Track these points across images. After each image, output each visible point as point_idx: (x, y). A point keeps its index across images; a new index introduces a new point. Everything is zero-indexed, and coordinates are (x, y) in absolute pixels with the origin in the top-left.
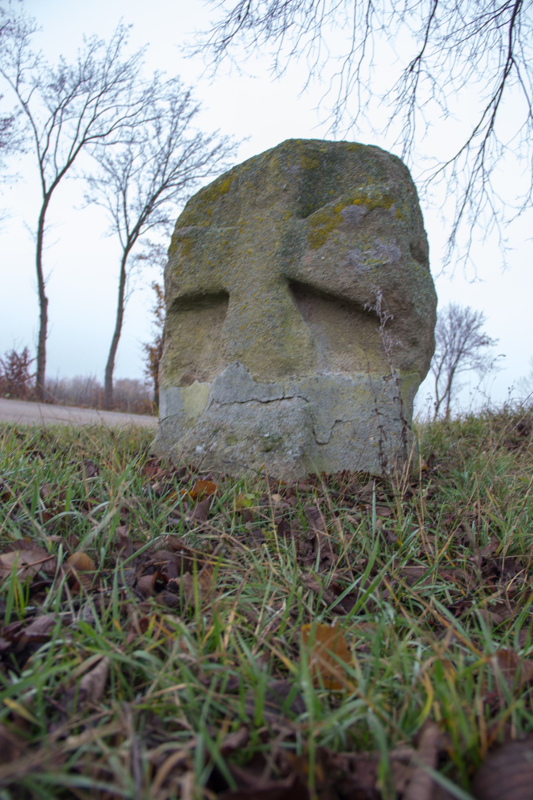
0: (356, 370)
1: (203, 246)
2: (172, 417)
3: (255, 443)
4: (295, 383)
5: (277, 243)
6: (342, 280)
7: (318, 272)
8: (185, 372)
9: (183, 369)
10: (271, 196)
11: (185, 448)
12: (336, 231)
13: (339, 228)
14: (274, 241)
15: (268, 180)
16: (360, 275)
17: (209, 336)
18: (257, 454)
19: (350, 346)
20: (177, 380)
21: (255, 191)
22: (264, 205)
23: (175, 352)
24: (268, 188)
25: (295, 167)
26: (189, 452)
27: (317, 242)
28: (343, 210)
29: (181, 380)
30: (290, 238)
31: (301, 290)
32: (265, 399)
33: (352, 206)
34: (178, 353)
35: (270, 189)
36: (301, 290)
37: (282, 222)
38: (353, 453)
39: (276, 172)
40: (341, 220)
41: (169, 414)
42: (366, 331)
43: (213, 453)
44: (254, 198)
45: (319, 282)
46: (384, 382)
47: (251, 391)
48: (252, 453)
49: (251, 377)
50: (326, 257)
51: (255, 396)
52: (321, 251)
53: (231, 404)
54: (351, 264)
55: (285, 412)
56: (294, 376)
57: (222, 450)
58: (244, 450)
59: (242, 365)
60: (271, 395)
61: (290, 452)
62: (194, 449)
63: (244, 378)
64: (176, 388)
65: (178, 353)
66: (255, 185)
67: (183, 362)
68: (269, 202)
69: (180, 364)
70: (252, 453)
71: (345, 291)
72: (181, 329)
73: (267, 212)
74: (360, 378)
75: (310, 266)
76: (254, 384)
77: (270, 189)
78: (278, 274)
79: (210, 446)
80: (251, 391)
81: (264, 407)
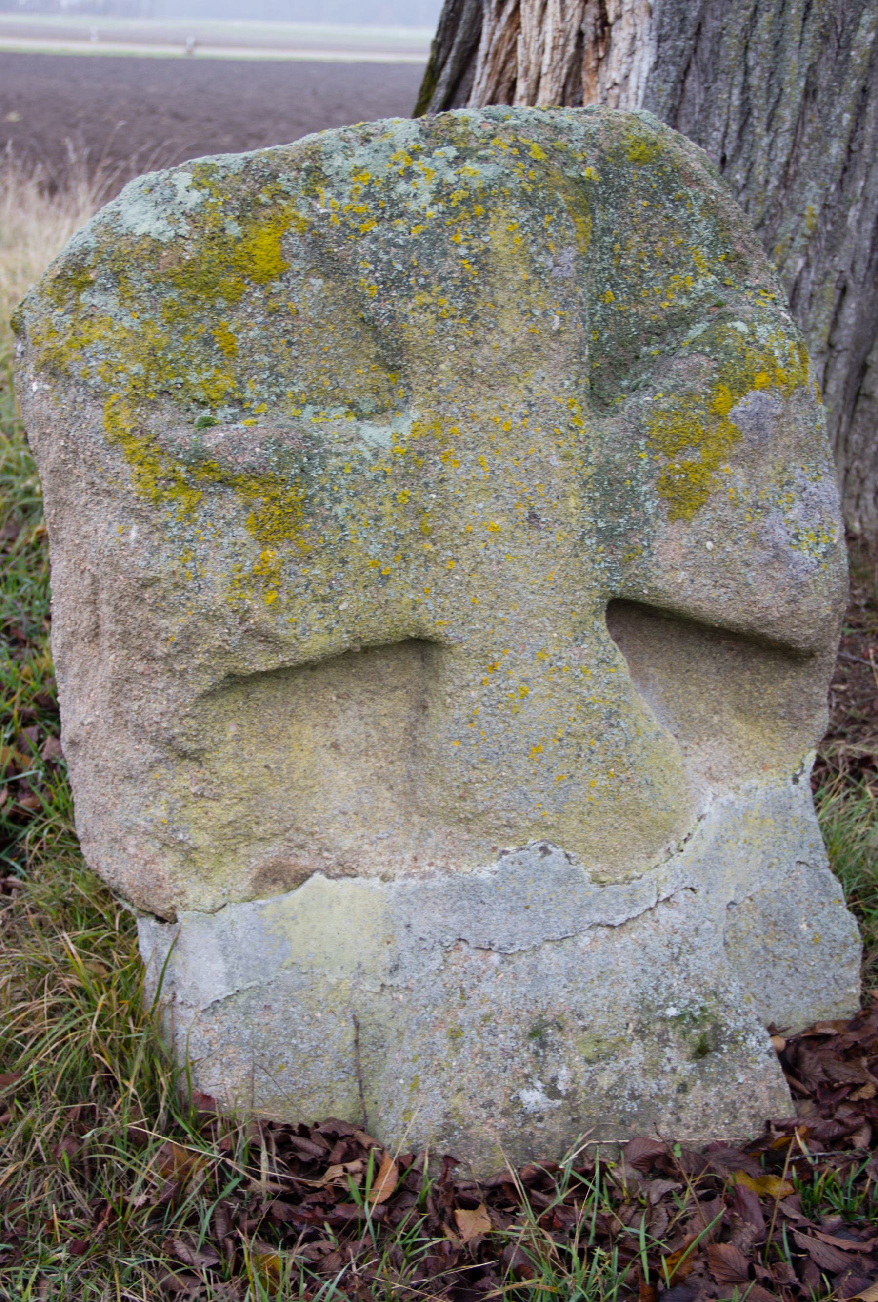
0: (738, 775)
1: (339, 510)
2: (258, 992)
3: (664, 1041)
4: (677, 861)
5: (572, 502)
7: (700, 580)
9: (260, 848)
10: (520, 350)
12: (726, 467)
13: (735, 460)
15: (501, 297)
17: (335, 746)
18: (686, 1068)
19: (716, 718)
20: (245, 886)
21: (466, 333)
22: (499, 376)
23: (228, 808)
24: (506, 325)
25: (568, 255)
26: (505, 1113)
27: (683, 498)
28: (737, 409)
30: (610, 490)
31: (634, 615)
32: (620, 919)
33: (752, 394)
34: (241, 808)
35: (513, 326)
36: (634, 615)
37: (572, 437)
38: (779, 972)
40: (735, 437)
41: (239, 984)
42: (752, 682)
43: (571, 1096)
44: (467, 353)
45: (706, 606)
46: (793, 787)
48: (674, 1070)
49: (587, 875)
50: (719, 544)
51: (597, 918)
55: (678, 938)
57: (592, 1083)
58: (653, 1069)
59: (557, 852)
60: (634, 903)
61: (752, 1042)
62: (517, 1102)
63: (567, 880)
64: (248, 906)
65: (241, 808)
66: (467, 311)
67: (259, 831)
68: (515, 368)
69: (248, 836)
70: (674, 1070)
71: (769, 624)
72: (238, 739)
73: (513, 398)
74: (748, 792)
75: (678, 568)
76: (595, 888)
77: (513, 326)
79: (554, 1080)
81: (628, 938)
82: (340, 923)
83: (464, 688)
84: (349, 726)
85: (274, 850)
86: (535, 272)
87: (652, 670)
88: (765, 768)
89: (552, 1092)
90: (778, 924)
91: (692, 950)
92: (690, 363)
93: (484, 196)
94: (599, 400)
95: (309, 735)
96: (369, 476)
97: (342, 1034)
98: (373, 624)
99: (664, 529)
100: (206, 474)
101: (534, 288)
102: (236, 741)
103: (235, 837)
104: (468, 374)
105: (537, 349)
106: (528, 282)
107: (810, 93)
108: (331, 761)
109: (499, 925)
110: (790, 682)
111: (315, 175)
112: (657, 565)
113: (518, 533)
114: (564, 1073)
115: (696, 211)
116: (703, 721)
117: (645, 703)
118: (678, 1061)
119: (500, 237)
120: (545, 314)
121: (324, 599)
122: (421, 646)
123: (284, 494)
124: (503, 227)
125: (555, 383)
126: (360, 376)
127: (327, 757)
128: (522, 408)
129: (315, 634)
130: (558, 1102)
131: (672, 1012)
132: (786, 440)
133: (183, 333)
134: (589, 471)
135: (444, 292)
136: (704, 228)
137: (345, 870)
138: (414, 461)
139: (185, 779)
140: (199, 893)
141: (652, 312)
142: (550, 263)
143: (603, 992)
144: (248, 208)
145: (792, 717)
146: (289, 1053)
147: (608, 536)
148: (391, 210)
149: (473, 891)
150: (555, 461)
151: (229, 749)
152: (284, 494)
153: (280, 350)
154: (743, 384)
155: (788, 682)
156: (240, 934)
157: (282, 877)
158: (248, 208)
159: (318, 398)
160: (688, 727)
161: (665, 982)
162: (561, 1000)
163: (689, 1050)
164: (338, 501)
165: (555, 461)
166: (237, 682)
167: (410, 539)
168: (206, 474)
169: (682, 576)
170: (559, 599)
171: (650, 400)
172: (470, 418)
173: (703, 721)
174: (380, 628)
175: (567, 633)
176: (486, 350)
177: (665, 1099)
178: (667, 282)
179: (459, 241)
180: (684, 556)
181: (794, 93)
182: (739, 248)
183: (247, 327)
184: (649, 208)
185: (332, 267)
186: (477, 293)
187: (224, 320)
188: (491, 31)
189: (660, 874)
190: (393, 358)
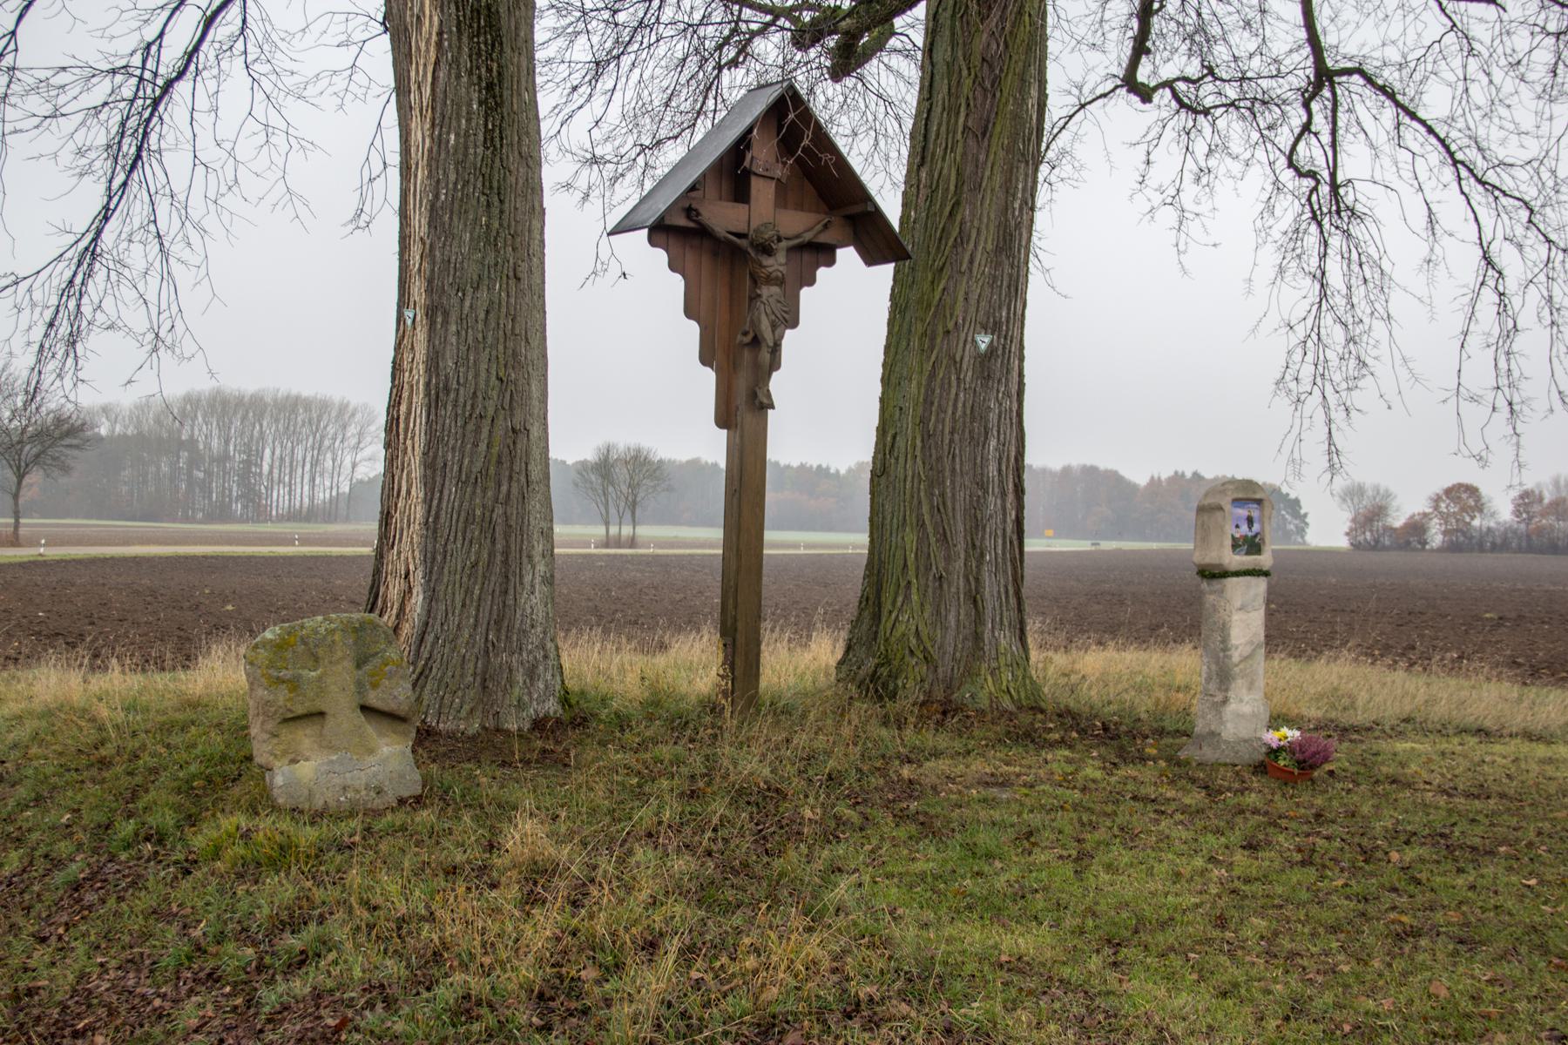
8: (292, 756)
22: (338, 662)
27: (375, 686)
31: (366, 709)
35: (339, 654)
36: (366, 709)
75: (373, 699)
77: (339, 654)
82: (306, 770)
83: (330, 722)
84: (308, 731)
90: (402, 776)
92: (377, 661)
93: (334, 630)
94: (358, 666)
95: (300, 733)
97: (306, 792)
100: (280, 681)
102: (284, 730)
103: (285, 753)
107: (463, 605)
108: (304, 737)
109: (337, 768)
110: (402, 727)
111: (302, 627)
117: (370, 729)
118: (373, 794)
119: (337, 637)
122: (322, 714)
123: (294, 684)
125: (348, 664)
126: (310, 664)
129: (300, 710)
137: (307, 760)
138: (320, 679)
139: (275, 741)
140: (278, 764)
141: (372, 651)
144: (289, 634)
145: (405, 734)
148: (316, 633)
149: (332, 762)
152: (294, 684)
157: (294, 761)
158: (289, 634)
159: (303, 668)
160: (381, 734)
162: (349, 782)
166: (286, 720)
168: (280, 681)
171: (367, 668)
174: (313, 710)
179: (329, 638)
181: (459, 606)
183: (289, 655)
185: (305, 644)
188: (382, 589)
189: (371, 759)
190: (317, 659)
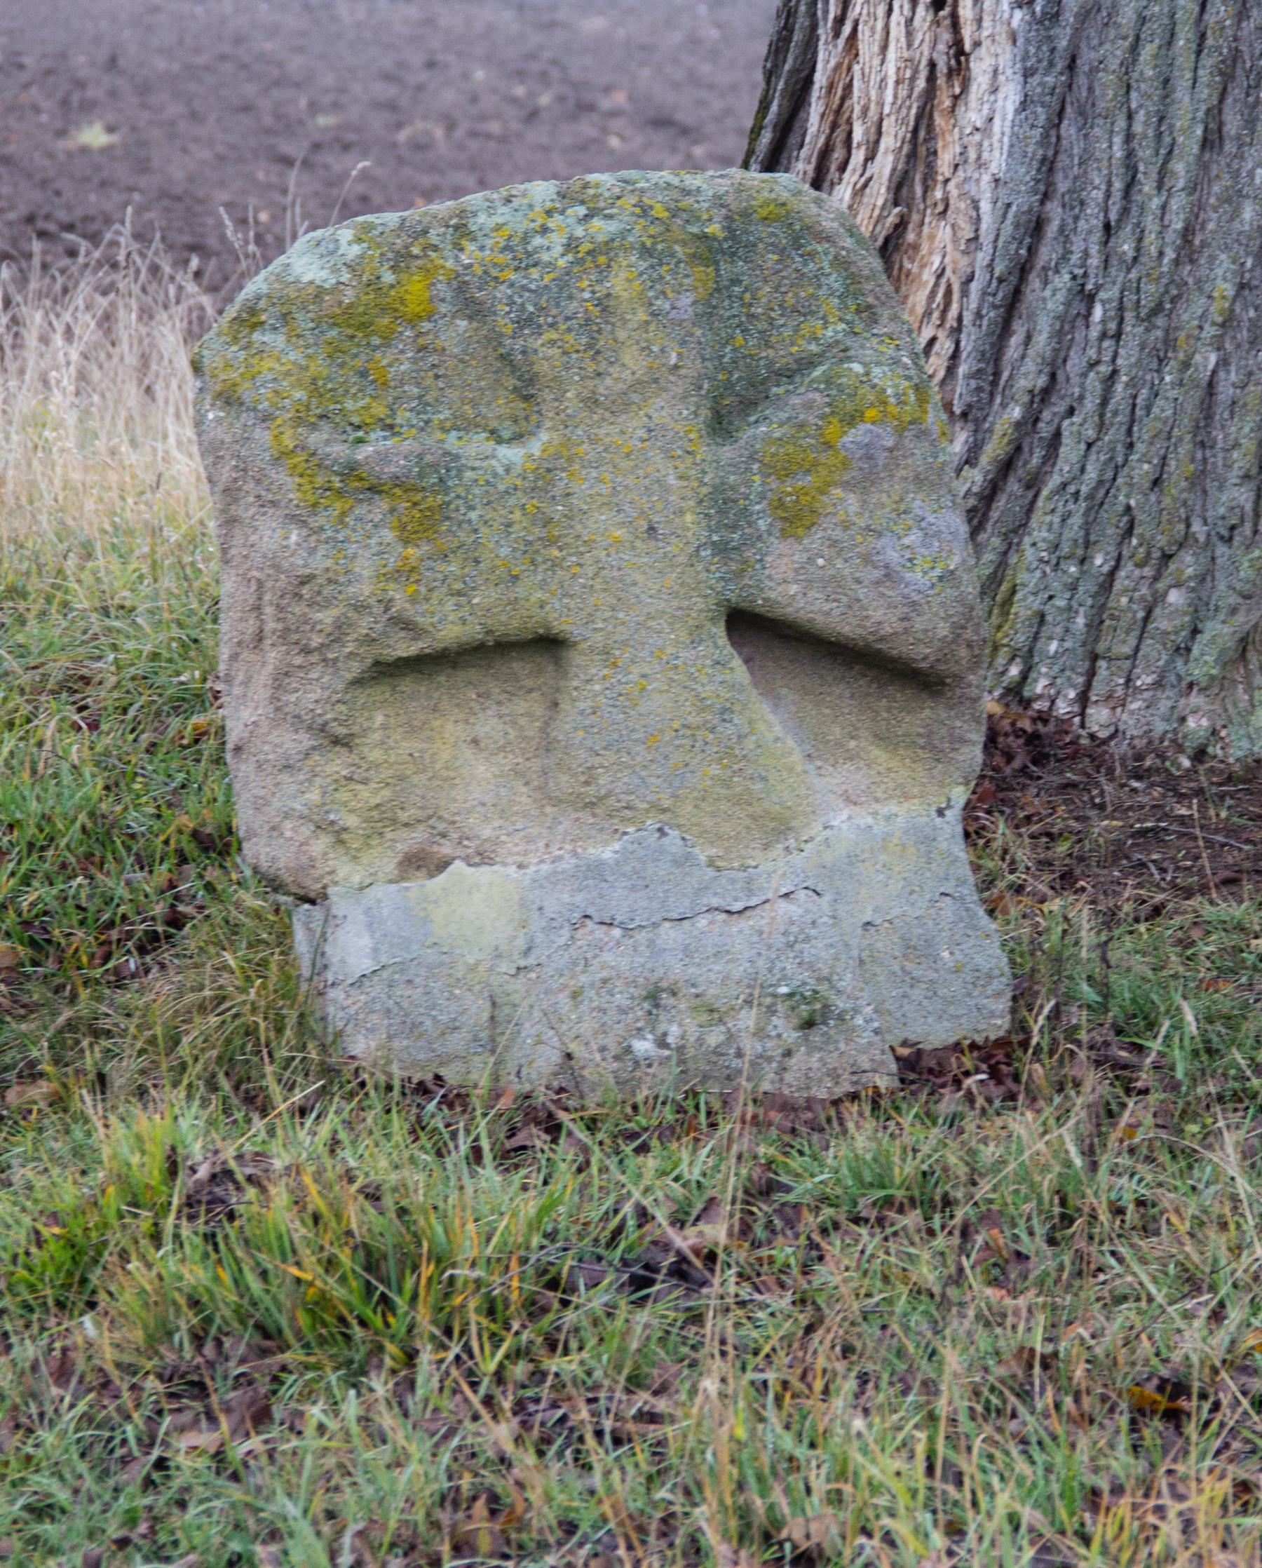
0: (877, 800)
1: (473, 515)
2: (402, 967)
3: (771, 1011)
4: (796, 858)
5: (689, 518)
6: (878, 615)
7: (812, 594)
9: (404, 833)
10: (639, 382)
11: (603, 1049)
12: (837, 492)
13: (846, 485)
14: (681, 512)
15: (622, 335)
16: (914, 603)
17: (475, 741)
18: (791, 1036)
19: (852, 744)
20: (389, 867)
21: (591, 367)
22: (620, 405)
24: (627, 359)
25: (686, 300)
27: (795, 518)
28: (846, 439)
29: (400, 864)
30: (724, 507)
32: (738, 906)
33: (862, 427)
34: (386, 793)
35: (633, 362)
37: (689, 460)
38: (917, 993)
39: (642, 315)
40: (845, 465)
41: (384, 959)
42: (889, 710)
43: (681, 1049)
44: (590, 383)
45: (820, 619)
46: (939, 820)
47: (702, 890)
49: (703, 858)
50: (829, 561)
51: (715, 902)
52: (815, 540)
53: (655, 925)
54: (889, 576)
55: (794, 929)
56: (792, 842)
57: (700, 1041)
58: (760, 1033)
59: (674, 833)
60: (750, 892)
61: (859, 1021)
62: (628, 1050)
63: (684, 861)
64: (393, 887)
65: (386, 793)
66: (590, 346)
67: (403, 816)
68: (635, 397)
69: (394, 821)
71: (882, 639)
72: (384, 727)
73: (634, 425)
74: (888, 818)
76: (711, 872)
77: (633, 362)
78: (712, 601)
79: (665, 1034)
80: (702, 890)
81: (744, 924)
82: (479, 906)
83: (588, 681)
84: (488, 725)
85: (418, 837)
86: (653, 314)
87: (784, 691)
88: (907, 797)
89: (662, 1043)
90: (917, 949)
91: (807, 939)
92: (803, 400)
95: (451, 729)
96: (501, 488)
97: (478, 1010)
98: (503, 618)
99: (777, 545)
100: (360, 484)
101: (652, 327)
102: (381, 721)
103: (383, 821)
104: (592, 402)
105: (656, 381)
106: (647, 323)
107: (1211, 141)
108: (469, 749)
109: (620, 902)
111: (461, 231)
112: (769, 577)
113: (638, 544)
114: (674, 1030)
115: (826, 264)
116: (839, 744)
117: (772, 721)
118: (784, 1028)
119: (623, 281)
120: (662, 351)
121: (459, 593)
122: (549, 645)
123: (424, 502)
124: (623, 275)
125: (675, 412)
126: (500, 406)
127: (468, 752)
128: (641, 433)
129: (451, 625)
130: (667, 1053)
131: (784, 990)
132: (903, 473)
133: (342, 366)
134: (705, 490)
135: (569, 330)
136: (834, 281)
137: (483, 858)
138: (542, 478)
139: (337, 764)
140: (347, 872)
141: (782, 356)
142: (667, 306)
143: (717, 968)
144: (401, 260)
145: (936, 750)
146: (428, 1022)
147: (722, 549)
148: (526, 261)
149: (597, 871)
150: (672, 480)
151: (377, 736)
152: (424, 502)
153: (428, 382)
154: (853, 418)
155: (927, 712)
156: (385, 913)
157: (423, 863)
158: (401, 260)
159: (464, 425)
160: (821, 750)
161: (779, 965)
162: (676, 970)
163: (796, 1021)
164: (472, 508)
165: (672, 480)
166: (387, 671)
167: (538, 545)
168: (360, 484)
169: (793, 589)
170: (675, 603)
171: (763, 431)
172: (593, 441)
173: (839, 744)
174: (511, 623)
175: (684, 636)
176: (608, 381)
177: (770, 1059)
178: (797, 329)
179: (585, 286)
180: (796, 570)
181: (1189, 141)
182: (870, 300)
183: (398, 361)
184: (779, 262)
185: (475, 310)
186: (599, 331)
187: (378, 355)
188: (827, 58)
189: (777, 868)
190: (527, 388)
